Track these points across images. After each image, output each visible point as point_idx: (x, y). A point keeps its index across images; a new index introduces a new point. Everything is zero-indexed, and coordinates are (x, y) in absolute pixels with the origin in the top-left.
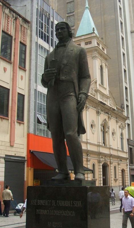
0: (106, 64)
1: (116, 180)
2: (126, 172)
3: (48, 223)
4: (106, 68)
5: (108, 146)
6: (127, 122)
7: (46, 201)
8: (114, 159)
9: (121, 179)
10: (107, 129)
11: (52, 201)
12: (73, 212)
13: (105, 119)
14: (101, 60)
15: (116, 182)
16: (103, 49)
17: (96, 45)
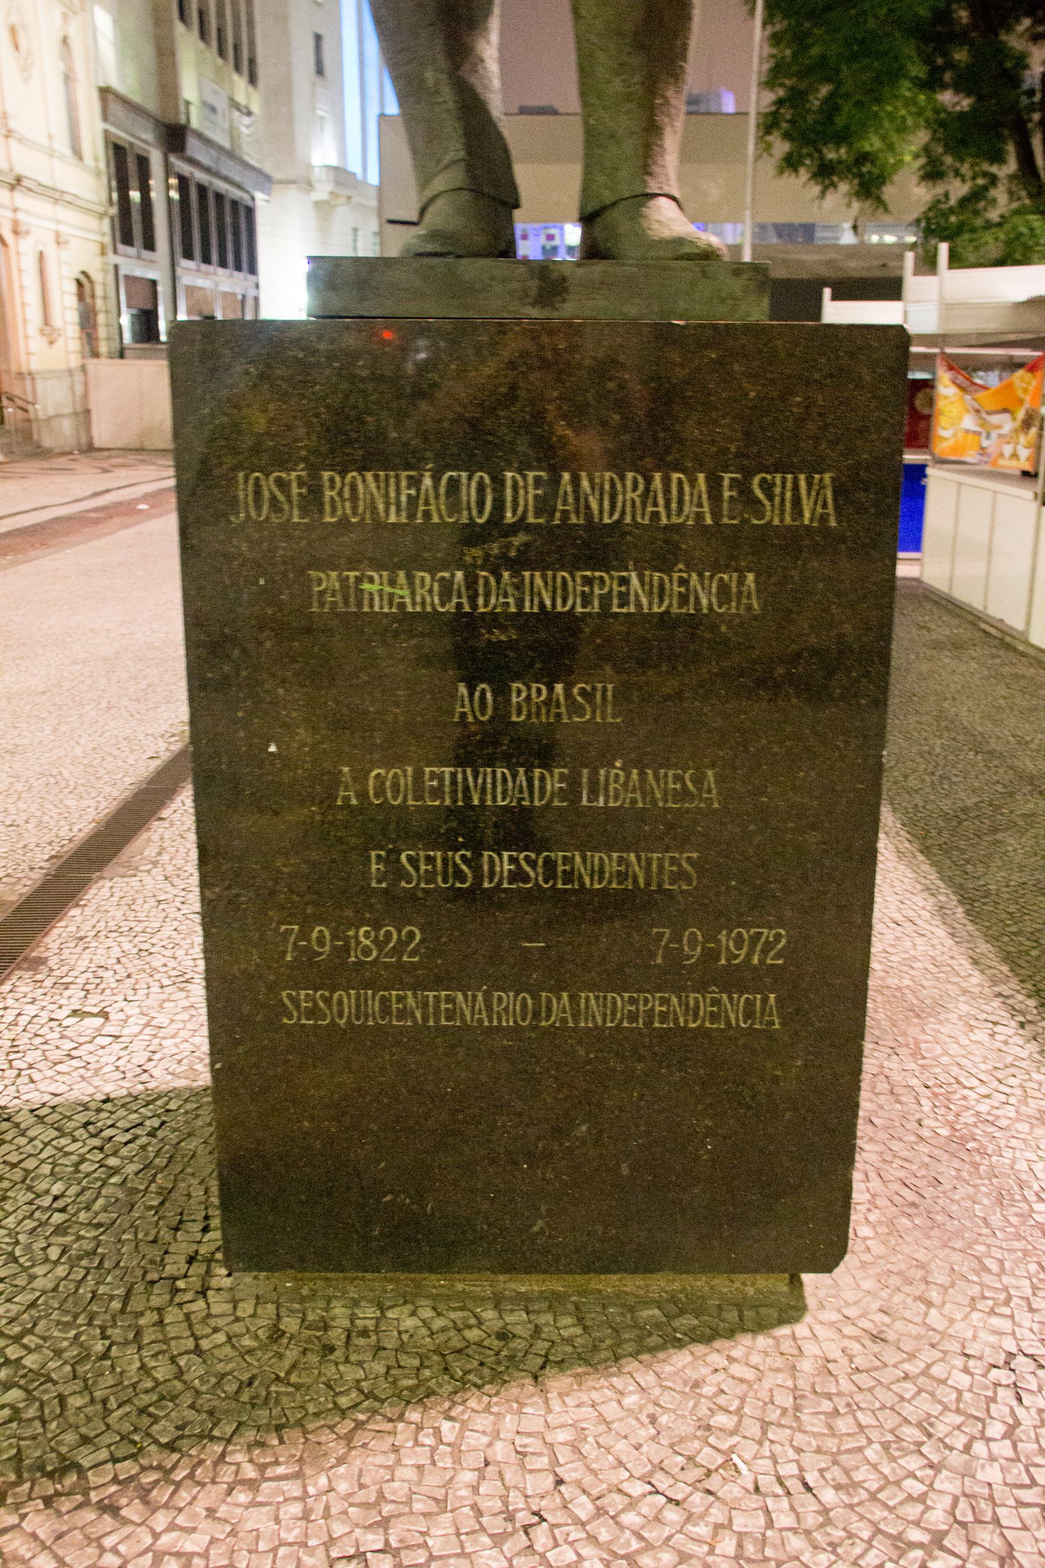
7: (427, 482)
11: (498, 482)
12: (741, 582)
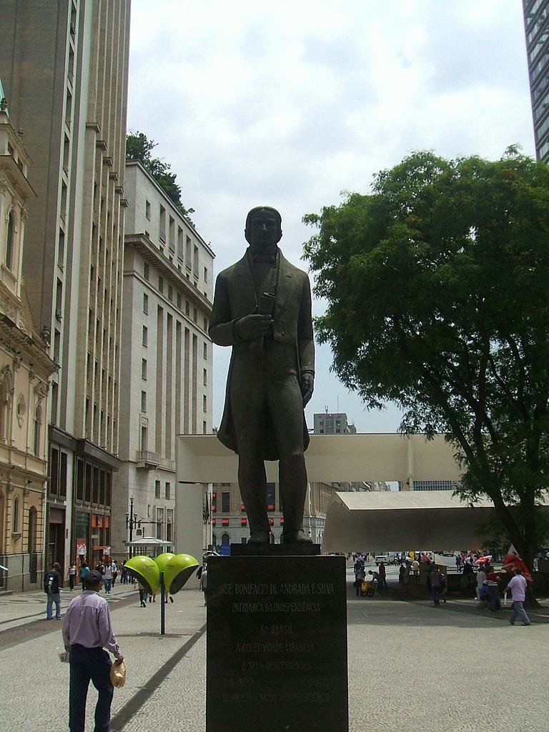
0: (22, 210)
1: (16, 537)
2: (39, 515)
3: (262, 627)
4: (21, 220)
5: (6, 443)
6: (56, 378)
8: (17, 479)
9: (26, 534)
10: (8, 395)
13: (8, 366)
14: (13, 197)
15: (15, 541)
16: (20, 166)
17: (7, 153)
